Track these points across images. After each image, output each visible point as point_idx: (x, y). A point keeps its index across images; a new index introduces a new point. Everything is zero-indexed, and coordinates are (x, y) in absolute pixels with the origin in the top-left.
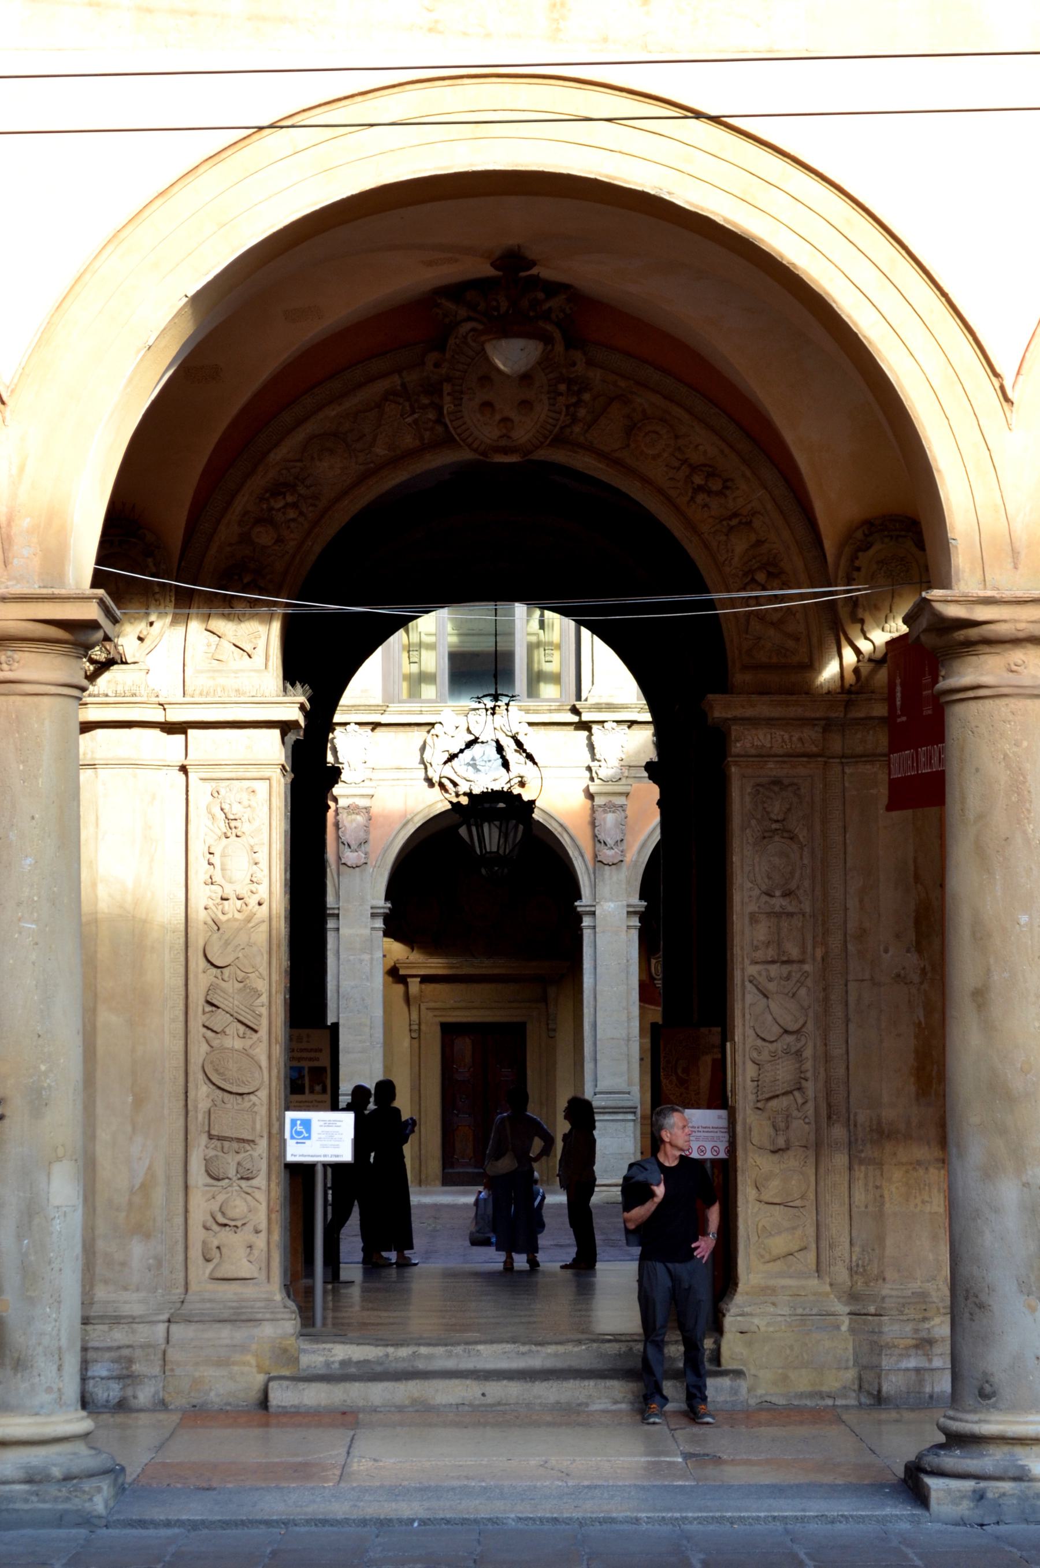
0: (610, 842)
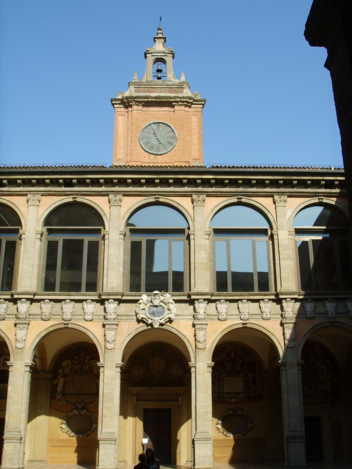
0: (201, 341)
